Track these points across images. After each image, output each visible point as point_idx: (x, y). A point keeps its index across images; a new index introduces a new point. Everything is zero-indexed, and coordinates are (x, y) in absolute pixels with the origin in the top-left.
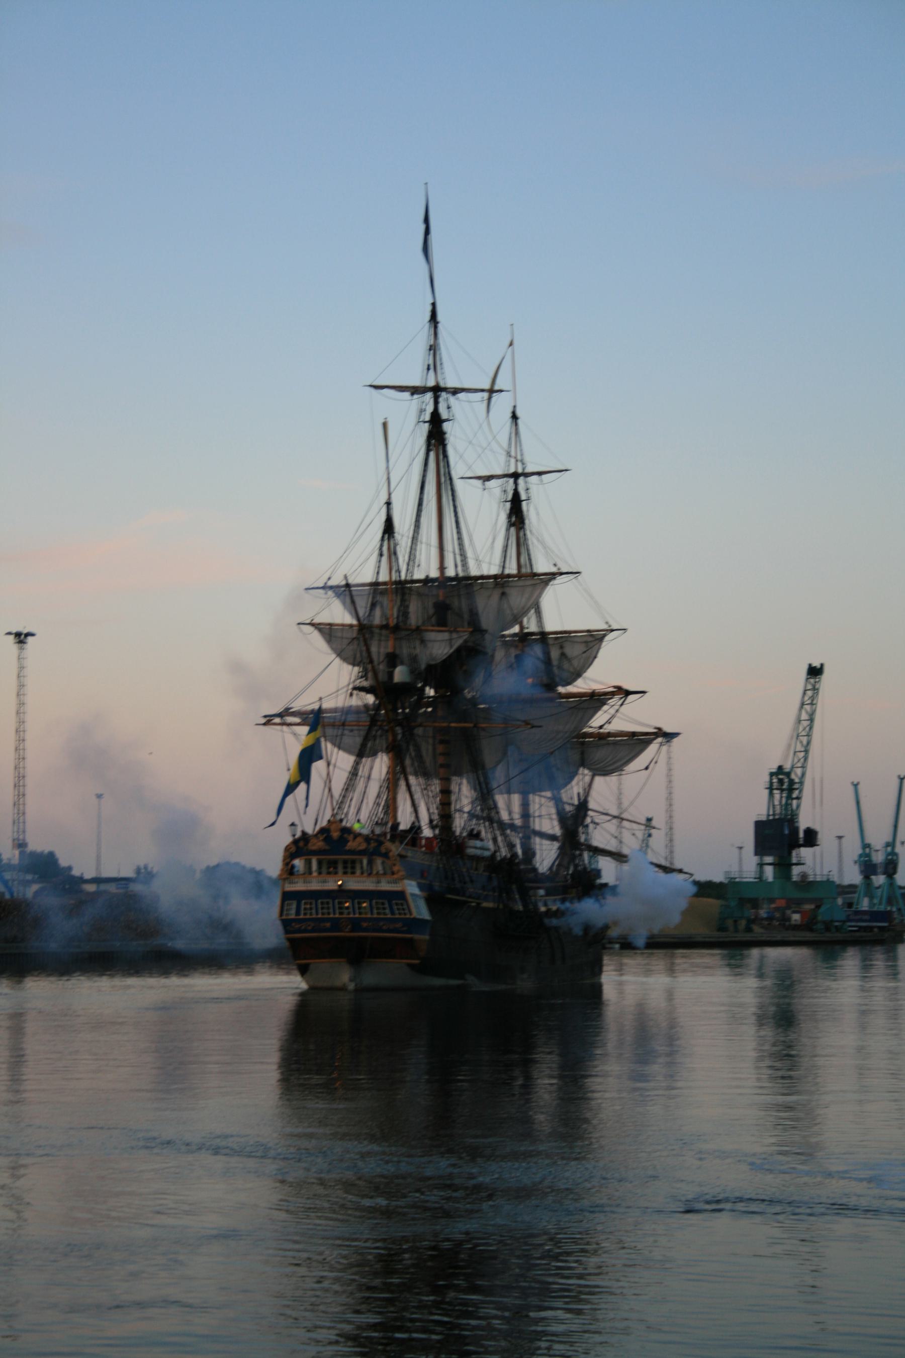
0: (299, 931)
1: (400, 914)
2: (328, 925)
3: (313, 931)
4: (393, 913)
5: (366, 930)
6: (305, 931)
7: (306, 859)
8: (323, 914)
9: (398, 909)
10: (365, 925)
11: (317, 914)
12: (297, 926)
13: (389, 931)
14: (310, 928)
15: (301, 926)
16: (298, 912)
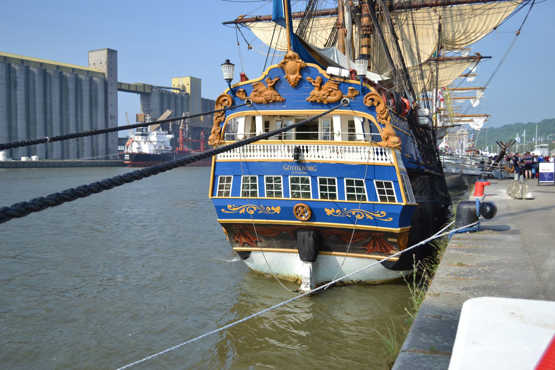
0: (237, 215)
1: (383, 199)
2: (277, 210)
3: (256, 216)
4: (373, 197)
5: (331, 219)
6: (246, 216)
7: (246, 117)
8: (270, 194)
9: (381, 192)
10: (329, 212)
11: (262, 194)
12: (234, 209)
13: (365, 221)
14: (252, 212)
15: (239, 210)
16: (236, 192)
